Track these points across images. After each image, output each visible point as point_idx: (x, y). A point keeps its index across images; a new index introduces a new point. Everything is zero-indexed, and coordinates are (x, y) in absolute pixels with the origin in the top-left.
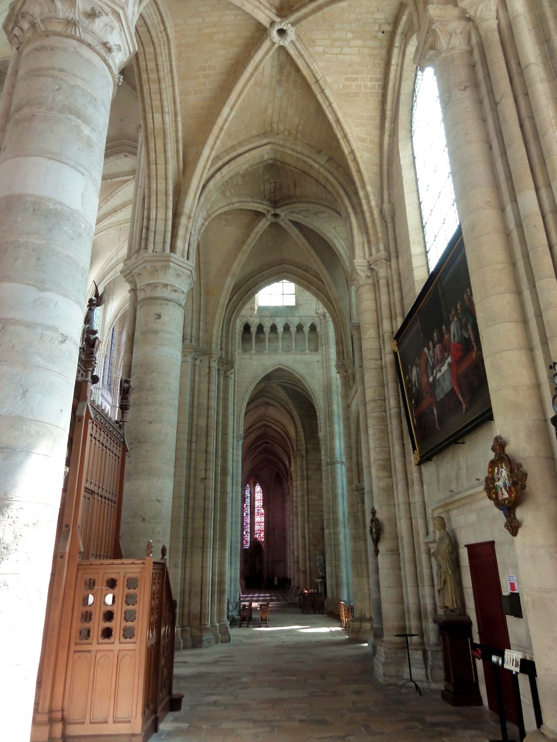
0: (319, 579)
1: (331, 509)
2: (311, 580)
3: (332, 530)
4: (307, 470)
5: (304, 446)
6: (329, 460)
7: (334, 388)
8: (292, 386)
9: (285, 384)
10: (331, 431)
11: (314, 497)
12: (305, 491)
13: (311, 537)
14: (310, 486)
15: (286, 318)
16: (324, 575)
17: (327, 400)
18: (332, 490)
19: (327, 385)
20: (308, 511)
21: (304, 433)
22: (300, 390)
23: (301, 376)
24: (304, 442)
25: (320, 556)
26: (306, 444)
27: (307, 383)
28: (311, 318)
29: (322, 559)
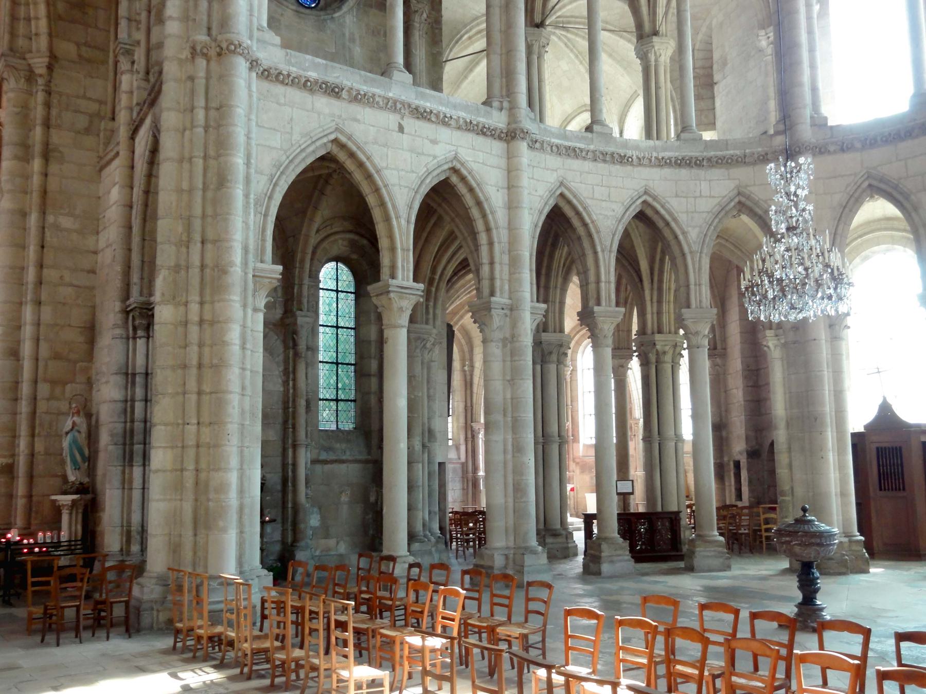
0: (65, 493)
1: (197, 224)
2: (30, 497)
3: (194, 308)
4: (47, 125)
5: (43, 42)
6: (202, 38)
11: (66, 222)
12: (35, 198)
13: (44, 351)
14: (53, 183)
16: (86, 480)
18: (205, 158)
20: (40, 266)
24: (43, 24)
26: (50, 35)
29: (84, 428)
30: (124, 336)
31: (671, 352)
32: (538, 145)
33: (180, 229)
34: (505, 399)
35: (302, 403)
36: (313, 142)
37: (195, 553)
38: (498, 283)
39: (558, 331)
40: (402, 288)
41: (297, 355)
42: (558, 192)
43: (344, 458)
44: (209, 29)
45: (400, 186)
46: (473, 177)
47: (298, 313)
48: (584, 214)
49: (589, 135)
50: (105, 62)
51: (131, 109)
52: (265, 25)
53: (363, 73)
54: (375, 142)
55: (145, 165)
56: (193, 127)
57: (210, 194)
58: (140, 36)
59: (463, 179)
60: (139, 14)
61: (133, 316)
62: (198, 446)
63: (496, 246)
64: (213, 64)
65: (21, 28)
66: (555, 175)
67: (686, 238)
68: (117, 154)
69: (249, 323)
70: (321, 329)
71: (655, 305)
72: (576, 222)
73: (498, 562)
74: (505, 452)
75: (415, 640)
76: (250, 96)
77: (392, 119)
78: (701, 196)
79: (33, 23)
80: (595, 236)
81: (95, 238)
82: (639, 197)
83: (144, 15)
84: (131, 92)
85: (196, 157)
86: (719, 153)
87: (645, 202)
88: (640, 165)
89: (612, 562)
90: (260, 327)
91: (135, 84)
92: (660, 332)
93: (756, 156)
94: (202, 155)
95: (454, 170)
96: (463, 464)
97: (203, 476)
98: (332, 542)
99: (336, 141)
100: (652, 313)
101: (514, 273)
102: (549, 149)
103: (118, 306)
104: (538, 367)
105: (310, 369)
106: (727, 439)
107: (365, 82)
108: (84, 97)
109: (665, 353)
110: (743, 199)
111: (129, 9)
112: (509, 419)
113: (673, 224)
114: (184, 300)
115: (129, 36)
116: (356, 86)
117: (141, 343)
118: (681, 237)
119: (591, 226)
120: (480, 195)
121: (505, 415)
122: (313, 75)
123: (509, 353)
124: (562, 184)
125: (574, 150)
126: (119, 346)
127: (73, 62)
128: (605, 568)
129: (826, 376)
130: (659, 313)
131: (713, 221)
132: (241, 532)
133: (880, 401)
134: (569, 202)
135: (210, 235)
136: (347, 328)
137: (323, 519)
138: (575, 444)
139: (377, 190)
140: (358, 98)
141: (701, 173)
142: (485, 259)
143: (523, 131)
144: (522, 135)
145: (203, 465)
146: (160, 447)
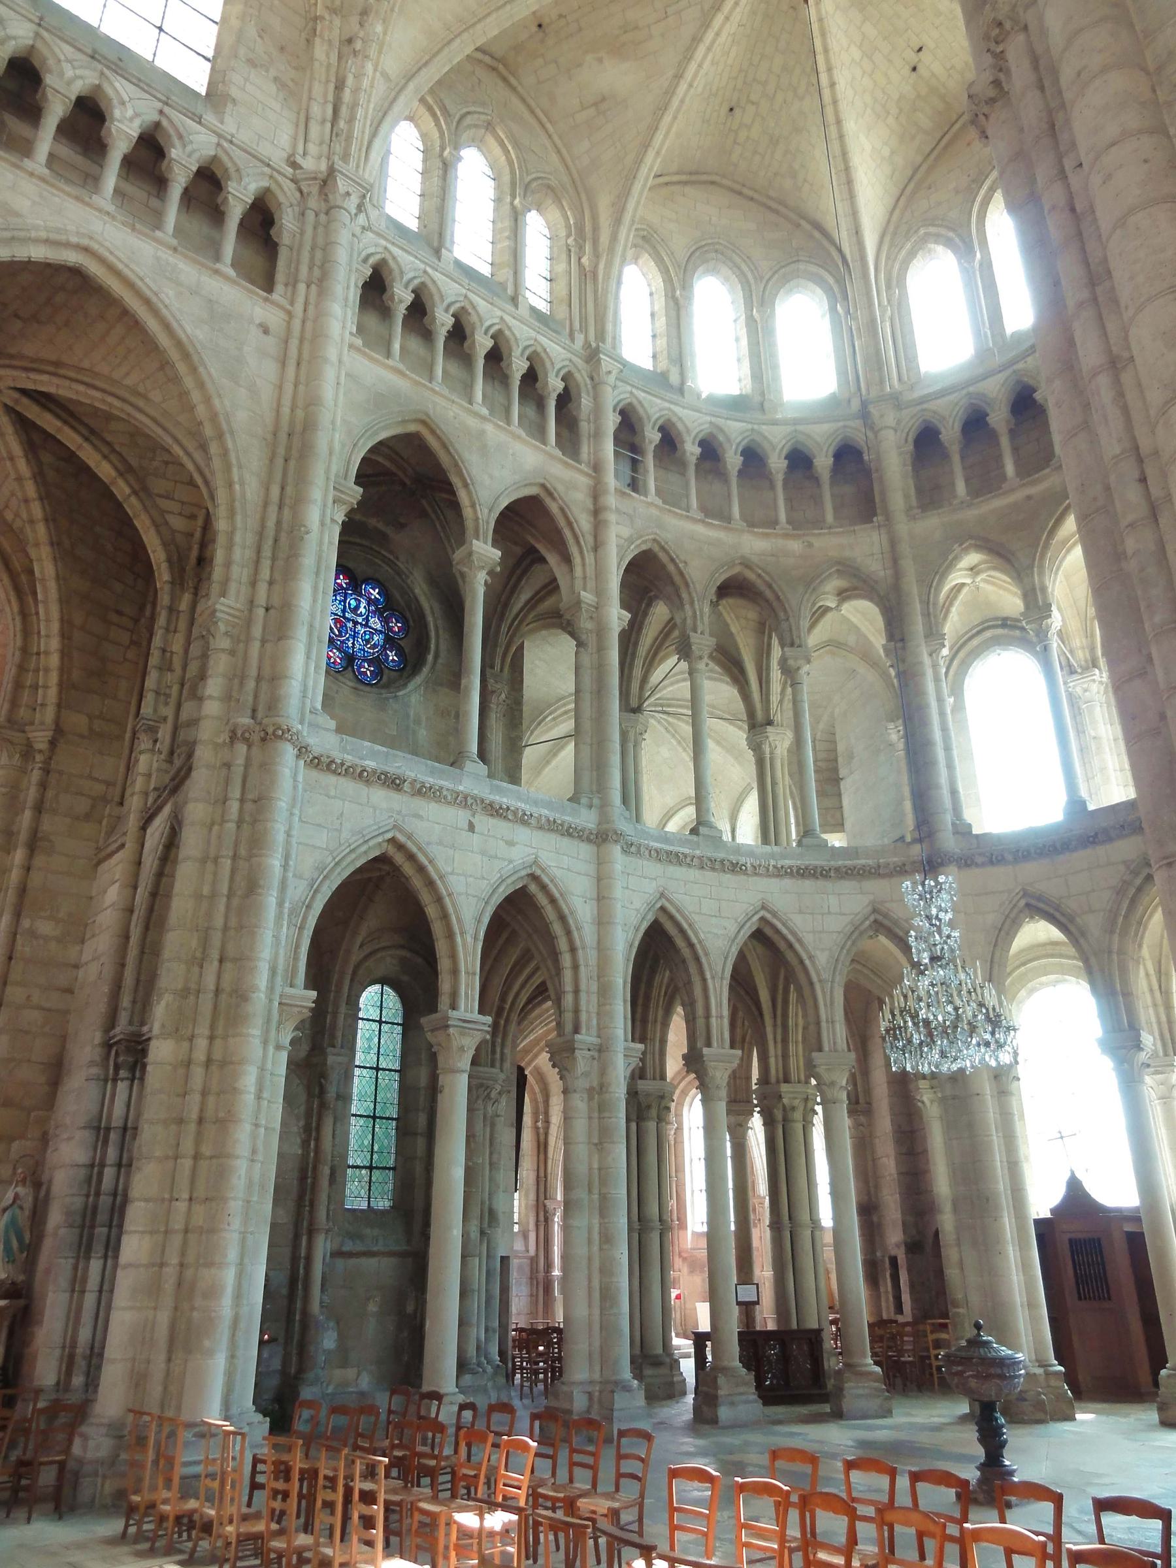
1: (216, 939)
3: (202, 1043)
4: (39, 809)
5: (50, 714)
6: (246, 721)
7: (322, 441)
8: (70, 438)
9: (48, 422)
10: (276, 601)
11: (46, 928)
14: (36, 879)
15: (159, 105)
16: (21, 1278)
17: (278, 476)
18: (235, 857)
19: (292, 423)
21: (62, 658)
22: (105, 470)
23: (179, 344)
24: (52, 693)
25: (20, 1189)
26: (59, 706)
27: (201, 385)
28: (267, 170)
29: (28, 1203)
30: (102, 1077)
31: (802, 1108)
32: (633, 849)
33: (194, 943)
34: (590, 1169)
35: (326, 1171)
36: (366, 842)
37: (165, 1388)
38: (583, 1017)
39: (658, 1077)
40: (465, 1021)
41: (323, 1105)
42: (658, 905)
43: (375, 1249)
44: (254, 711)
45: (467, 895)
46: (556, 886)
47: (329, 1050)
48: (690, 933)
49: (694, 838)
50: (120, 738)
51: (146, 794)
52: (319, 707)
53: (429, 762)
54: (440, 843)
55: (156, 862)
56: (223, 821)
57: (235, 902)
58: (168, 711)
59: (544, 887)
60: (170, 687)
61: (117, 1052)
62: (186, 1231)
63: (582, 969)
64: (255, 750)
65: (26, 696)
66: (654, 884)
67: (813, 963)
68: (123, 846)
69: (269, 1066)
70: (357, 1071)
71: (779, 1046)
72: (680, 942)
73: (579, 1403)
74: (590, 1241)
75: (468, 1519)
76: (295, 788)
77: (461, 816)
78: (829, 913)
79: (40, 691)
80: (704, 960)
81: (78, 948)
82: (756, 913)
83: (175, 689)
84: (149, 775)
85: (222, 857)
86: (848, 863)
87: (762, 919)
88: (756, 874)
89: (732, 1404)
90: (282, 1070)
91: (155, 765)
92: (787, 1080)
93: (892, 866)
94: (231, 854)
95: (534, 877)
96: (532, 1259)
97: (189, 1273)
98: (351, 1373)
99: (393, 841)
100: (776, 1056)
101: (604, 1005)
102: (647, 853)
103: (98, 1037)
104: (634, 1126)
105: (338, 1125)
106: (880, 1225)
107: (432, 773)
108: (90, 777)
109: (793, 1108)
110: (880, 918)
111: (159, 682)
112: (596, 1197)
113: (797, 946)
114: (189, 1033)
115: (155, 710)
116: (421, 778)
117: (122, 1086)
118: (807, 962)
119: (698, 946)
120: (564, 907)
121: (590, 1191)
122: (370, 764)
123: (595, 1106)
124: (662, 895)
125: (677, 855)
126: (93, 1091)
127: (82, 736)
128: (724, 1413)
129: (996, 1141)
130: (785, 1056)
131: (845, 943)
132: (232, 1357)
133: (1068, 1175)
134: (671, 918)
135: (231, 951)
136: (390, 1070)
137: (341, 1338)
138: (681, 1232)
139: (439, 900)
140: (422, 791)
141: (828, 885)
142: (568, 987)
143: (616, 833)
144: (614, 837)
145: (190, 1258)
146: (136, 1232)
